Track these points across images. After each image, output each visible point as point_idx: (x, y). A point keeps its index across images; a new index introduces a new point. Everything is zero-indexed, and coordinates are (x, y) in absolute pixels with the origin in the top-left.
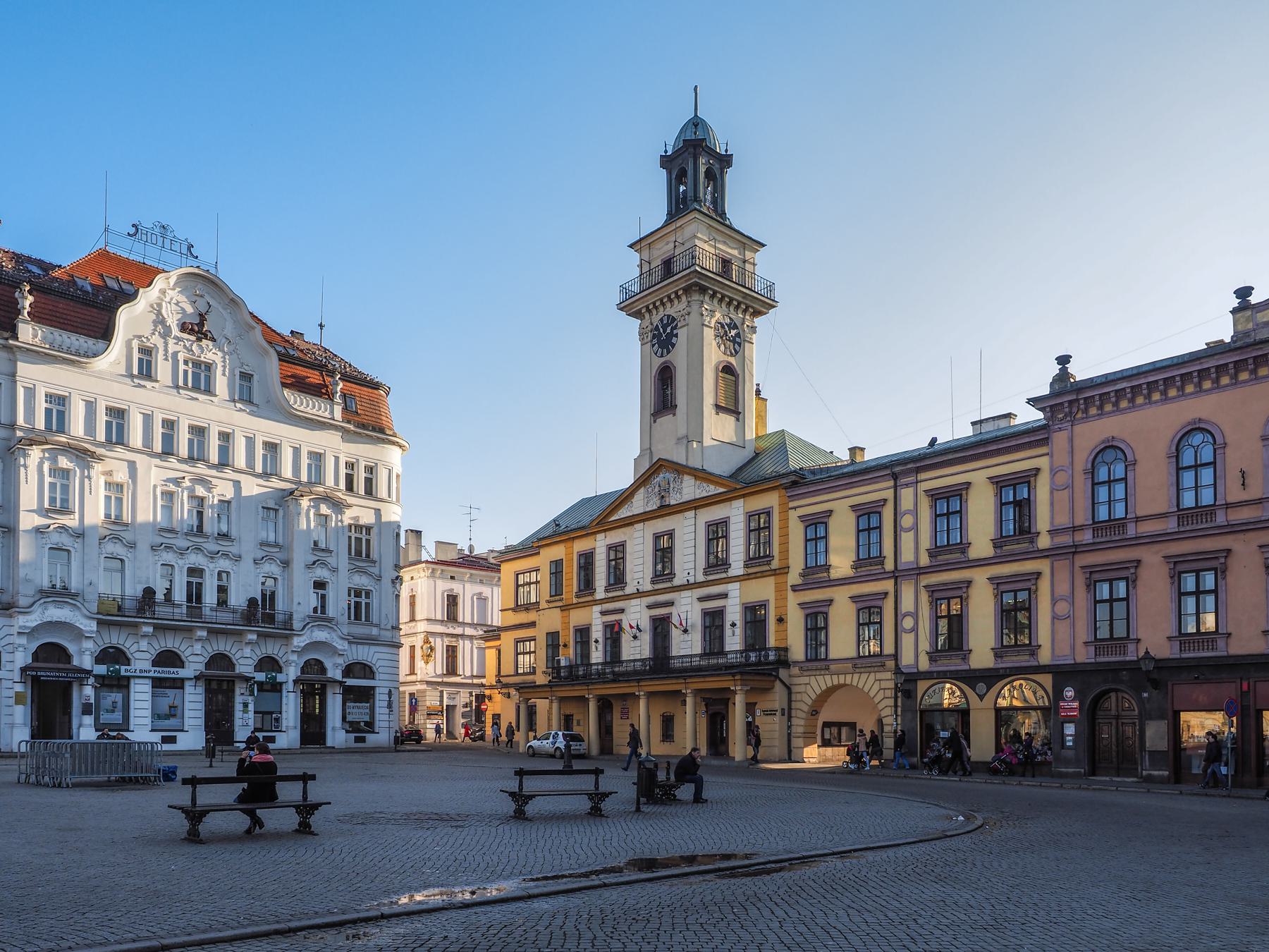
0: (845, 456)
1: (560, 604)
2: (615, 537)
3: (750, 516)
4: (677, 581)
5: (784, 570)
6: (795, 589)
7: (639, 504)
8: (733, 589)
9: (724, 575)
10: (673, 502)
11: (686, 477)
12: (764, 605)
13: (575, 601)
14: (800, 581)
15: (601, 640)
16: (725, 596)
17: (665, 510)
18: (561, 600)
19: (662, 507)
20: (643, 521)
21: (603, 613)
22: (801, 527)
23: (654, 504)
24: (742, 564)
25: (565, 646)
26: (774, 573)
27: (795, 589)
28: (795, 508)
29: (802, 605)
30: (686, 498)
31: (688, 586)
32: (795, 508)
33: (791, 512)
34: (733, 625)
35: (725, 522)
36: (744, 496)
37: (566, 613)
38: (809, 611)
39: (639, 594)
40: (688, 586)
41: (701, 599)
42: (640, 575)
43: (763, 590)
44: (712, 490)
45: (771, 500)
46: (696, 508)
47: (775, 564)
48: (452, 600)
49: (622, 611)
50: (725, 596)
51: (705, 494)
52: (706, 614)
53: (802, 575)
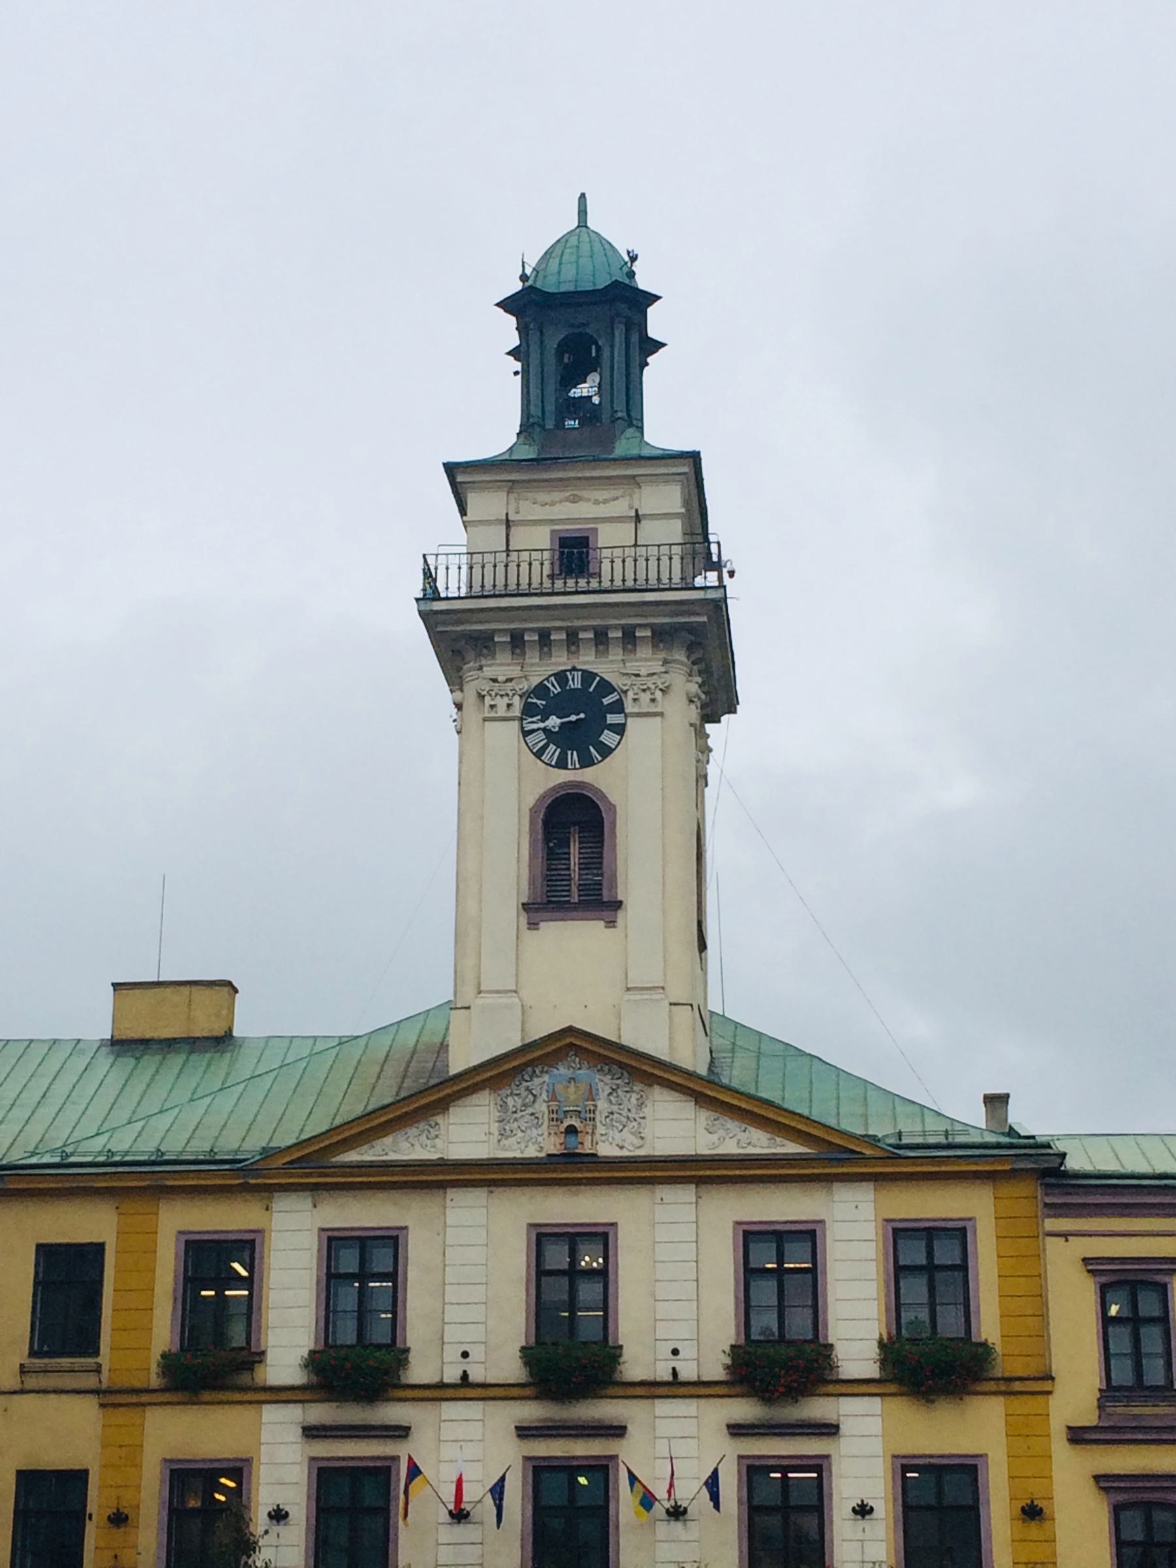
0: (975, 1116)
1: (90, 1381)
3: (900, 1234)
6: (1077, 1436)
7: (469, 1132)
10: (606, 1150)
14: (1088, 1416)
16: (830, 1430)
17: (572, 1167)
23: (535, 1142)
24: (873, 1351)
25: (119, 1519)
26: (1009, 1387)
27: (1077, 1436)
28: (1065, 1235)
29: (1104, 1482)
31: (674, 1387)
32: (1065, 1235)
33: (1053, 1245)
34: (863, 1511)
35: (809, 1236)
36: (877, 1179)
37: (121, 1417)
38: (1121, 1497)
40: (674, 1387)
42: (474, 1333)
43: (970, 1428)
45: (974, 1205)
46: (700, 1181)
50: (830, 1430)
51: (730, 1148)
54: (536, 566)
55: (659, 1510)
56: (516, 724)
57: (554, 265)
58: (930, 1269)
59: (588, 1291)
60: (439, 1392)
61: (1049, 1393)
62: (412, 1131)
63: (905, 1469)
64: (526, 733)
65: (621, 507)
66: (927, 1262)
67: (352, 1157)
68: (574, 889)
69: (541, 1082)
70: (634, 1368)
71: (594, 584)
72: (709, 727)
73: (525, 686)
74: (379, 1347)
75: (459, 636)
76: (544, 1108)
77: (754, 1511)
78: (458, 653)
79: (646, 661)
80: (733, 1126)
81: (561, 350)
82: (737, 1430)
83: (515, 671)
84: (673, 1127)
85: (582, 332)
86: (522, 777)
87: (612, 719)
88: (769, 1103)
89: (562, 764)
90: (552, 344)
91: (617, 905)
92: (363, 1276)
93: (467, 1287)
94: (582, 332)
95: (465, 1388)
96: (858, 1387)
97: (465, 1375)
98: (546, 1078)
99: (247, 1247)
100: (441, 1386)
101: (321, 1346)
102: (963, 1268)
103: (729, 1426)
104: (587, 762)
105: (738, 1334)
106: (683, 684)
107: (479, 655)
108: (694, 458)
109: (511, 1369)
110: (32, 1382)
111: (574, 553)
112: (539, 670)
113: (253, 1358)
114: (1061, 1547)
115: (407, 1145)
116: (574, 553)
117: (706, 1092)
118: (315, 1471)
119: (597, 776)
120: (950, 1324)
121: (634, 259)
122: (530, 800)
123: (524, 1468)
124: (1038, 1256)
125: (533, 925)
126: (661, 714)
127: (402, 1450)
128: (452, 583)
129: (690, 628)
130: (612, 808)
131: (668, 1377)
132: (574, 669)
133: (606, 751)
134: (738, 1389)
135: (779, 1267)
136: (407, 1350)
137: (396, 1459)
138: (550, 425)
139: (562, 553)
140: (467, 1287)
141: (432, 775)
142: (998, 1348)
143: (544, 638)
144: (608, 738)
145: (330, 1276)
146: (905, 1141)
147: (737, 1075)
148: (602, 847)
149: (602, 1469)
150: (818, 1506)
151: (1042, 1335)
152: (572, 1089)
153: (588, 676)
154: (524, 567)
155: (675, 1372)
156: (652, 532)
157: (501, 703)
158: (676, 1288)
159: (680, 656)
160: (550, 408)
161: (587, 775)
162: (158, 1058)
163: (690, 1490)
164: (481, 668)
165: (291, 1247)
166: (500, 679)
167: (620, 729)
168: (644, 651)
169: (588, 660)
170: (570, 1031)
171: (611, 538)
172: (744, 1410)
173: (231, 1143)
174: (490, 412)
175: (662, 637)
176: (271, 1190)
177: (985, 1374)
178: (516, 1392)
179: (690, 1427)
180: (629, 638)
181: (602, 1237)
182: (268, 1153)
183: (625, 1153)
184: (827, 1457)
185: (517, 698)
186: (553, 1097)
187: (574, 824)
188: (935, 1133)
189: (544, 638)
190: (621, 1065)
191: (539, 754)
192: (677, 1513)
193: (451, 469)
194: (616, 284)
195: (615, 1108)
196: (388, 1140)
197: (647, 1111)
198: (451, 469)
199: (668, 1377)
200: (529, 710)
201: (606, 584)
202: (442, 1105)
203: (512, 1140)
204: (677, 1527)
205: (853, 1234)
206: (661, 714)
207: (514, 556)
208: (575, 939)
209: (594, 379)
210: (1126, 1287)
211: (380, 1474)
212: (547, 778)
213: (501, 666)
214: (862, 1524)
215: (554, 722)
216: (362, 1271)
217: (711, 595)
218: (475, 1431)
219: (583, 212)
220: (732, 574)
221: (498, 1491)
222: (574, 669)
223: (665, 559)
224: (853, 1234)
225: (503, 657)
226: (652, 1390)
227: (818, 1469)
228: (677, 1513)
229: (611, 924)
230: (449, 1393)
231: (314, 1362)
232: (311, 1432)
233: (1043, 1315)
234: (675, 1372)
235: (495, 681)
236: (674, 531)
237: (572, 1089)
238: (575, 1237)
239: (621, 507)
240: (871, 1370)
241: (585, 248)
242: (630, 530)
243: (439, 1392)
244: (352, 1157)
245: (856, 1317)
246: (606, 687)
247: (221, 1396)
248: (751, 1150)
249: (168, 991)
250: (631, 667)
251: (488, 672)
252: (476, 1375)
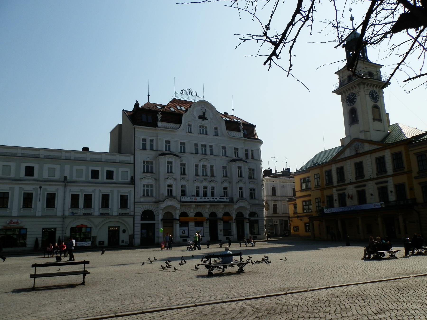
1: (320, 188)
2: (339, 165)
4: (366, 178)
5: (410, 172)
6: (416, 178)
8: (390, 180)
9: (384, 175)
10: (361, 152)
13: (325, 187)
15: (337, 200)
17: (358, 155)
18: (320, 187)
19: (356, 154)
24: (392, 171)
28: (412, 151)
29: (420, 184)
32: (412, 151)
34: (391, 192)
39: (351, 183)
41: (377, 184)
43: (403, 179)
44: (376, 147)
45: (401, 149)
46: (370, 153)
47: (406, 170)
48: (274, 189)
49: (345, 189)
50: (387, 182)
51: (373, 148)
52: (379, 188)
53: (418, 173)
56: (345, 103)
66: (397, 157)
80: (373, 145)
89: (351, 105)
104: (353, 104)
110: (316, 189)
112: (347, 94)
125: (350, 126)
133: (355, 102)
144: (355, 100)
153: (352, 93)
167: (356, 99)
170: (354, 139)
200: (347, 100)
208: (355, 126)
210: (420, 156)
212: (349, 108)
229: (358, 124)
244: (338, 159)
246: (354, 94)
252: (352, 181)
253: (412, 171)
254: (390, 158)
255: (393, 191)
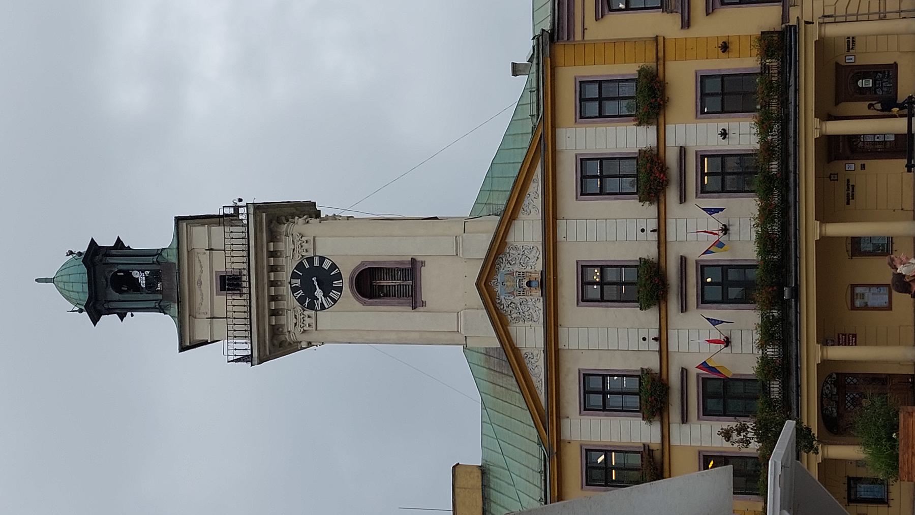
0: (523, 79)
6: (686, 24)
7: (530, 337)
10: (539, 267)
11: (510, 239)
12: (703, 79)
14: (677, 18)
16: (683, 151)
17: (548, 284)
20: (556, 325)
21: (685, 419)
22: (611, 18)
23: (535, 303)
24: (642, 129)
26: (661, 59)
27: (686, 24)
28: (584, 29)
29: (710, 10)
30: (538, 237)
31: (661, 231)
32: (584, 29)
34: (724, 134)
35: (583, 161)
36: (554, 127)
40: (661, 231)
44: (535, 188)
46: (555, 218)
50: (683, 151)
51: (538, 202)
54: (235, 303)
55: (724, 239)
57: (73, 295)
58: (600, 100)
59: (611, 276)
60: (664, 353)
61: (664, 38)
62: (529, 366)
63: (702, 112)
64: (323, 308)
65: (205, 258)
66: (597, 101)
67: (542, 398)
68: (405, 283)
69: (504, 299)
70: (650, 251)
71: (245, 272)
72: (323, 215)
73: (299, 308)
74: (640, 384)
75: (273, 344)
76: (517, 298)
77: (723, 190)
78: (281, 344)
79: (286, 245)
80: (526, 202)
81: (121, 292)
82: (683, 199)
83: (291, 314)
84: (528, 231)
85: (111, 280)
86: (347, 311)
87: (316, 264)
88: (515, 182)
89: (340, 289)
90: (116, 296)
91: (413, 261)
92: (604, 393)
93: (610, 338)
94: (111, 280)
95: (661, 339)
96: (661, 137)
97: (655, 339)
98: (502, 297)
99: (589, 452)
100: (660, 351)
101: (641, 414)
102: (600, 83)
103: (681, 203)
104: (339, 276)
105: (633, 199)
106: (299, 226)
107: (282, 333)
108: (178, 220)
109: (651, 316)
111: (229, 283)
112: (290, 301)
113: (647, 452)
114: (742, 33)
115: (536, 370)
116: (229, 283)
117: (509, 216)
118: (705, 417)
119: (347, 270)
120: (629, 90)
121: (71, 253)
122: (358, 305)
123: (703, 308)
124: (594, 43)
125: (424, 304)
126: (314, 238)
127: (694, 371)
128: (243, 347)
129: (269, 222)
130: (363, 263)
131: (656, 234)
132: (290, 283)
133: (334, 266)
134: (662, 198)
135: (598, 177)
136: (642, 370)
137: (698, 375)
138: (160, 297)
139: (229, 290)
140: (610, 338)
141: (343, 355)
142: (641, 64)
143: (273, 298)
144: (326, 265)
145: (604, 410)
146: (535, 113)
147: (501, 201)
148: (383, 268)
149: (703, 268)
150: (723, 157)
151: (635, 41)
152: (508, 284)
153: (294, 276)
154: (235, 309)
155: (654, 231)
156: (218, 243)
157: (307, 321)
158: (611, 230)
159: (284, 228)
160: (151, 297)
161: (346, 276)
162: (492, 504)
163: (713, 222)
164: (289, 332)
165: (587, 430)
166: (295, 321)
167: (322, 259)
168: (281, 246)
169: (285, 276)
171: (221, 266)
172: (672, 195)
173: (536, 464)
174: (154, 328)
175: (273, 237)
176: (559, 441)
177: (655, 71)
178: (663, 312)
179: (681, 222)
180: (273, 254)
181: (584, 268)
182: (541, 443)
183: (541, 256)
184: (696, 152)
185: (305, 313)
186: (512, 293)
187: (371, 283)
188: (531, 97)
189: (273, 298)
190: (496, 258)
191: (335, 301)
192: (725, 230)
193: (183, 348)
194: (84, 262)
195: (518, 262)
196: (534, 379)
197: (519, 245)
198: (183, 348)
199: (656, 234)
200: (311, 307)
201: (245, 266)
202: (516, 350)
203: (534, 315)
204: (732, 230)
205: (581, 139)
206: (314, 238)
207: (230, 314)
208: (431, 282)
209: (136, 274)
211: (705, 382)
213: (288, 321)
214: (731, 135)
215: (319, 293)
216: (599, 393)
217: (251, 211)
218: (684, 334)
219: (46, 280)
220: (240, 200)
221: (714, 322)
222: (290, 283)
223: (232, 235)
224: (581, 139)
225: (283, 320)
226: (662, 242)
227: (703, 157)
228: (725, 230)
229: (423, 263)
230: (664, 348)
231: (648, 417)
232: (685, 419)
233: (625, 41)
234: (654, 231)
235: (296, 324)
236: (217, 230)
237: (508, 284)
238: (584, 283)
239: (205, 258)
240: (652, 130)
241: (65, 278)
242: (218, 254)
243: (664, 353)
244: (542, 398)
245: (626, 138)
246: (300, 266)
247: (666, 466)
248: (540, 192)
249: (458, 500)
250: (289, 253)
251: (291, 328)
253: (656, 38)
254: (591, 130)
255: (723, 125)
